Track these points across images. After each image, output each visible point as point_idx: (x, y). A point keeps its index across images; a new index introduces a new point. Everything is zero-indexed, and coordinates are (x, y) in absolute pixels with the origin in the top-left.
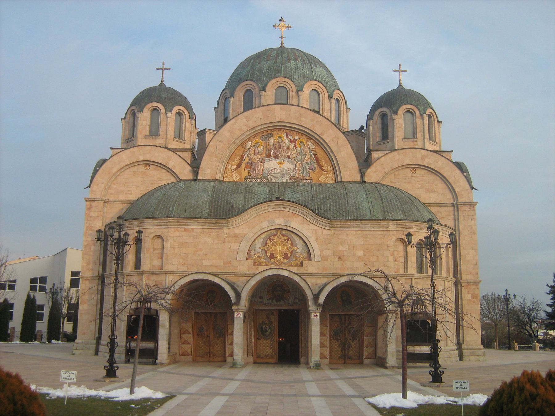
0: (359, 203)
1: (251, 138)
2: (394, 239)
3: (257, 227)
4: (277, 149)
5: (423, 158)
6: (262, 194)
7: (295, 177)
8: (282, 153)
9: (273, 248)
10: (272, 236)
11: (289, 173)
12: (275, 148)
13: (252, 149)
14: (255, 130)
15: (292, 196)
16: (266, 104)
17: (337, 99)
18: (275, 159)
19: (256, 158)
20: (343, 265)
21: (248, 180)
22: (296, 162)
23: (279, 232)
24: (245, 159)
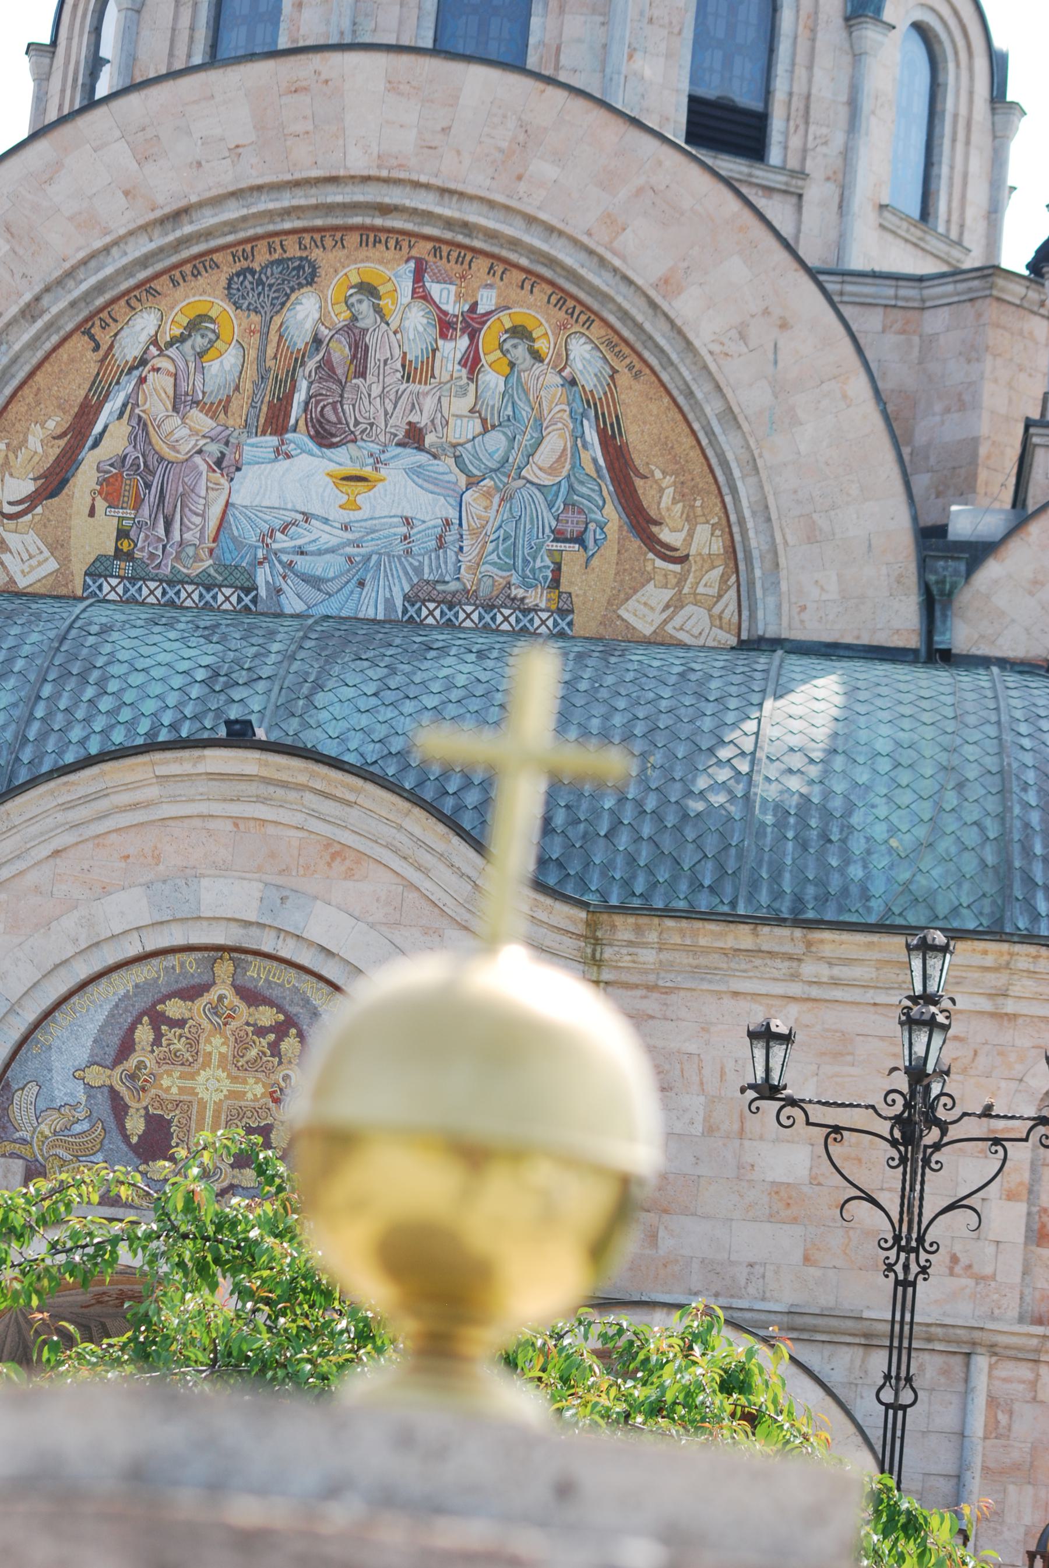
0: (836, 804)
1: (162, 284)
3: (69, 922)
4: (340, 371)
6: (156, 689)
7: (453, 586)
9: (171, 1083)
10: (169, 996)
11: (408, 552)
12: (326, 366)
13: (163, 363)
14: (188, 229)
15: (364, 720)
16: (367, 39)
17: (920, 28)
18: (311, 445)
21: (111, 588)
22: (469, 475)
23: (224, 969)
24: (102, 434)
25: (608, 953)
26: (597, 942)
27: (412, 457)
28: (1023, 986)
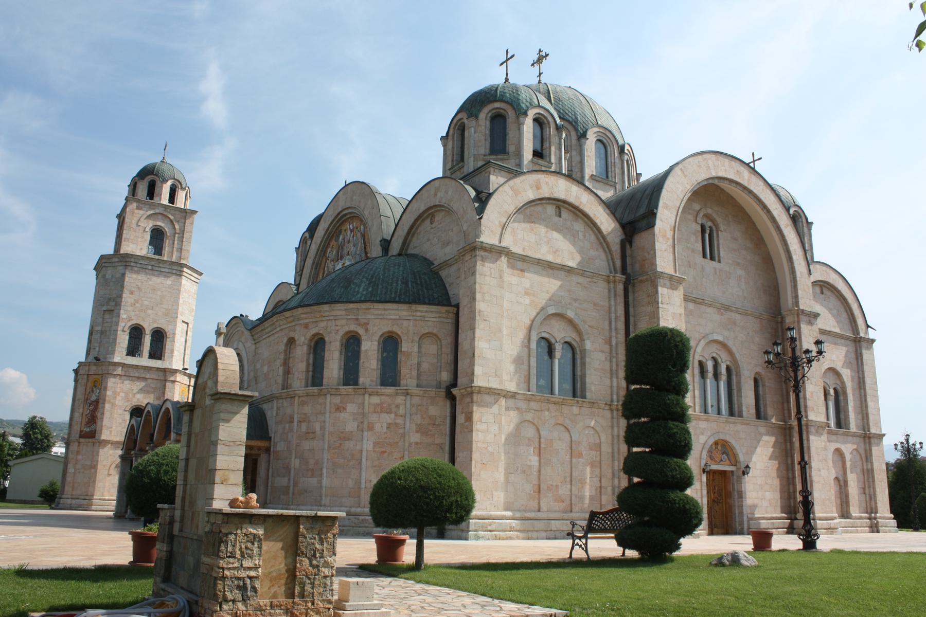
2: (285, 340)
5: (435, 195)
8: (345, 252)
26: (252, 336)
28: (281, 323)
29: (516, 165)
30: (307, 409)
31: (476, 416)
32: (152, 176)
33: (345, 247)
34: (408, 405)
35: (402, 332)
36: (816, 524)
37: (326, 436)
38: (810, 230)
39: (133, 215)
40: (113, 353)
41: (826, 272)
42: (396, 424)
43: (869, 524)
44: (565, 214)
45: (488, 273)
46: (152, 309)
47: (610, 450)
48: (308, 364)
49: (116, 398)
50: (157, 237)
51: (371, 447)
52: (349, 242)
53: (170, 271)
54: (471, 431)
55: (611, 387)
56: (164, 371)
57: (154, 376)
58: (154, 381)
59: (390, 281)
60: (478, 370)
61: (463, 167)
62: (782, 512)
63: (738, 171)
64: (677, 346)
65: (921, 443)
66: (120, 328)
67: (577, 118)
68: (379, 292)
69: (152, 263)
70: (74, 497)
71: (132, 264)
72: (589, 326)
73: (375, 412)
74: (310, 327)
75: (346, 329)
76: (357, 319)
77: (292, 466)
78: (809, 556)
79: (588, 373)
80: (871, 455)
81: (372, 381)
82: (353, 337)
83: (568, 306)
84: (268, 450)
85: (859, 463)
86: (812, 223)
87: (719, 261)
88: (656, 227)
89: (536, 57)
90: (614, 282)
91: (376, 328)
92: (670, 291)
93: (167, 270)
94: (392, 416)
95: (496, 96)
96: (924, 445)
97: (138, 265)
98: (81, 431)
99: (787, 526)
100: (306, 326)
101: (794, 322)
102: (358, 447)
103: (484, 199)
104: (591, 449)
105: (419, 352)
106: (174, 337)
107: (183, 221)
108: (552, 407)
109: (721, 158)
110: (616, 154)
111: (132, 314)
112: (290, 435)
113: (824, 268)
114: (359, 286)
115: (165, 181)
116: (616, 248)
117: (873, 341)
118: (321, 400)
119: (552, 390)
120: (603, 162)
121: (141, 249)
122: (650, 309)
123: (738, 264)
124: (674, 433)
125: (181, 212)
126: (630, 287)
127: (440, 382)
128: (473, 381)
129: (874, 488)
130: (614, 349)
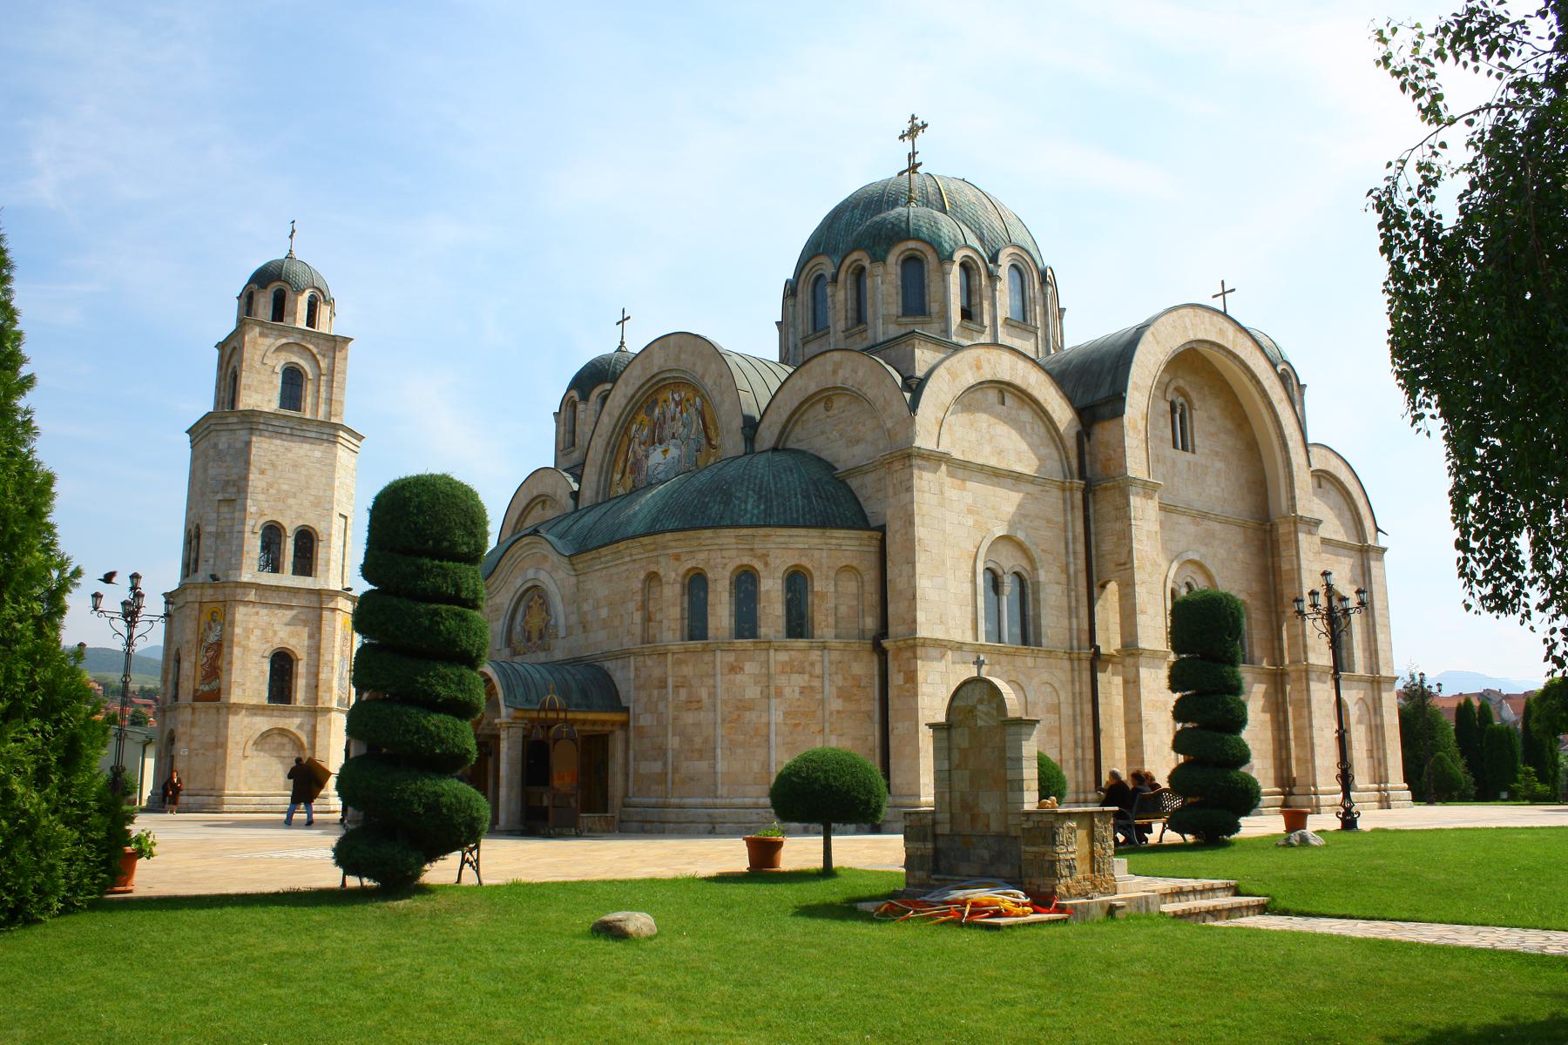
2: (642, 575)
5: (835, 372)
8: (667, 432)
19: (641, 451)
20: (587, 639)
25: (576, 567)
26: (573, 565)
27: (674, 441)
28: (634, 551)
29: (942, 331)
30: (687, 670)
31: (921, 676)
32: (279, 283)
33: (666, 426)
34: (826, 663)
35: (813, 567)
36: (1318, 800)
37: (719, 706)
38: (1302, 395)
39: (254, 347)
40: (239, 567)
41: (1326, 457)
42: (812, 688)
43: (1377, 799)
44: (1009, 399)
45: (927, 489)
46: (295, 496)
47: (1070, 712)
48: (683, 609)
49: (248, 637)
50: (293, 381)
51: (780, 720)
52: (673, 419)
53: (318, 436)
54: (916, 695)
55: (1070, 629)
56: (319, 593)
57: (304, 603)
58: (306, 610)
59: (787, 495)
60: (921, 617)
61: (866, 331)
62: (1276, 786)
63: (1220, 329)
64: (1232, 613)
65: (1439, 685)
66: (248, 528)
67: (983, 234)
68: (775, 512)
69: (290, 425)
70: (191, 792)
71: (261, 427)
72: (1043, 550)
73: (783, 672)
74: (683, 558)
75: (738, 562)
76: (752, 550)
77: (670, 746)
78: (1348, 836)
79: (1043, 612)
80: (1381, 706)
81: (777, 631)
82: (746, 571)
83: (1018, 526)
84: (625, 725)
85: (1366, 718)
86: (1305, 386)
87: (1193, 452)
88: (1126, 417)
89: (907, 127)
90: (1071, 489)
91: (778, 561)
92: (1144, 500)
93: (314, 435)
94: (806, 677)
95: (909, 230)
96: (1443, 688)
97: (270, 428)
98: (196, 691)
99: (1280, 803)
100: (677, 558)
101: (1290, 533)
102: (764, 720)
103: (914, 386)
104: (1048, 712)
105: (836, 591)
106: (329, 541)
107: (331, 355)
108: (1003, 659)
109: (1199, 312)
110: (1037, 286)
111: (265, 505)
112: (661, 706)
113: (1323, 451)
114: (746, 502)
115: (301, 291)
116: (1071, 443)
117: (1384, 550)
118: (707, 657)
119: (1000, 636)
120: (1019, 297)
121: (270, 401)
122: (1118, 526)
123: (1217, 454)
124: (1232, 709)
125: (328, 340)
126: (1090, 496)
127: (863, 631)
128: (915, 631)
129: (1384, 750)
130: (1072, 578)
